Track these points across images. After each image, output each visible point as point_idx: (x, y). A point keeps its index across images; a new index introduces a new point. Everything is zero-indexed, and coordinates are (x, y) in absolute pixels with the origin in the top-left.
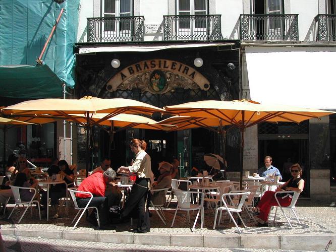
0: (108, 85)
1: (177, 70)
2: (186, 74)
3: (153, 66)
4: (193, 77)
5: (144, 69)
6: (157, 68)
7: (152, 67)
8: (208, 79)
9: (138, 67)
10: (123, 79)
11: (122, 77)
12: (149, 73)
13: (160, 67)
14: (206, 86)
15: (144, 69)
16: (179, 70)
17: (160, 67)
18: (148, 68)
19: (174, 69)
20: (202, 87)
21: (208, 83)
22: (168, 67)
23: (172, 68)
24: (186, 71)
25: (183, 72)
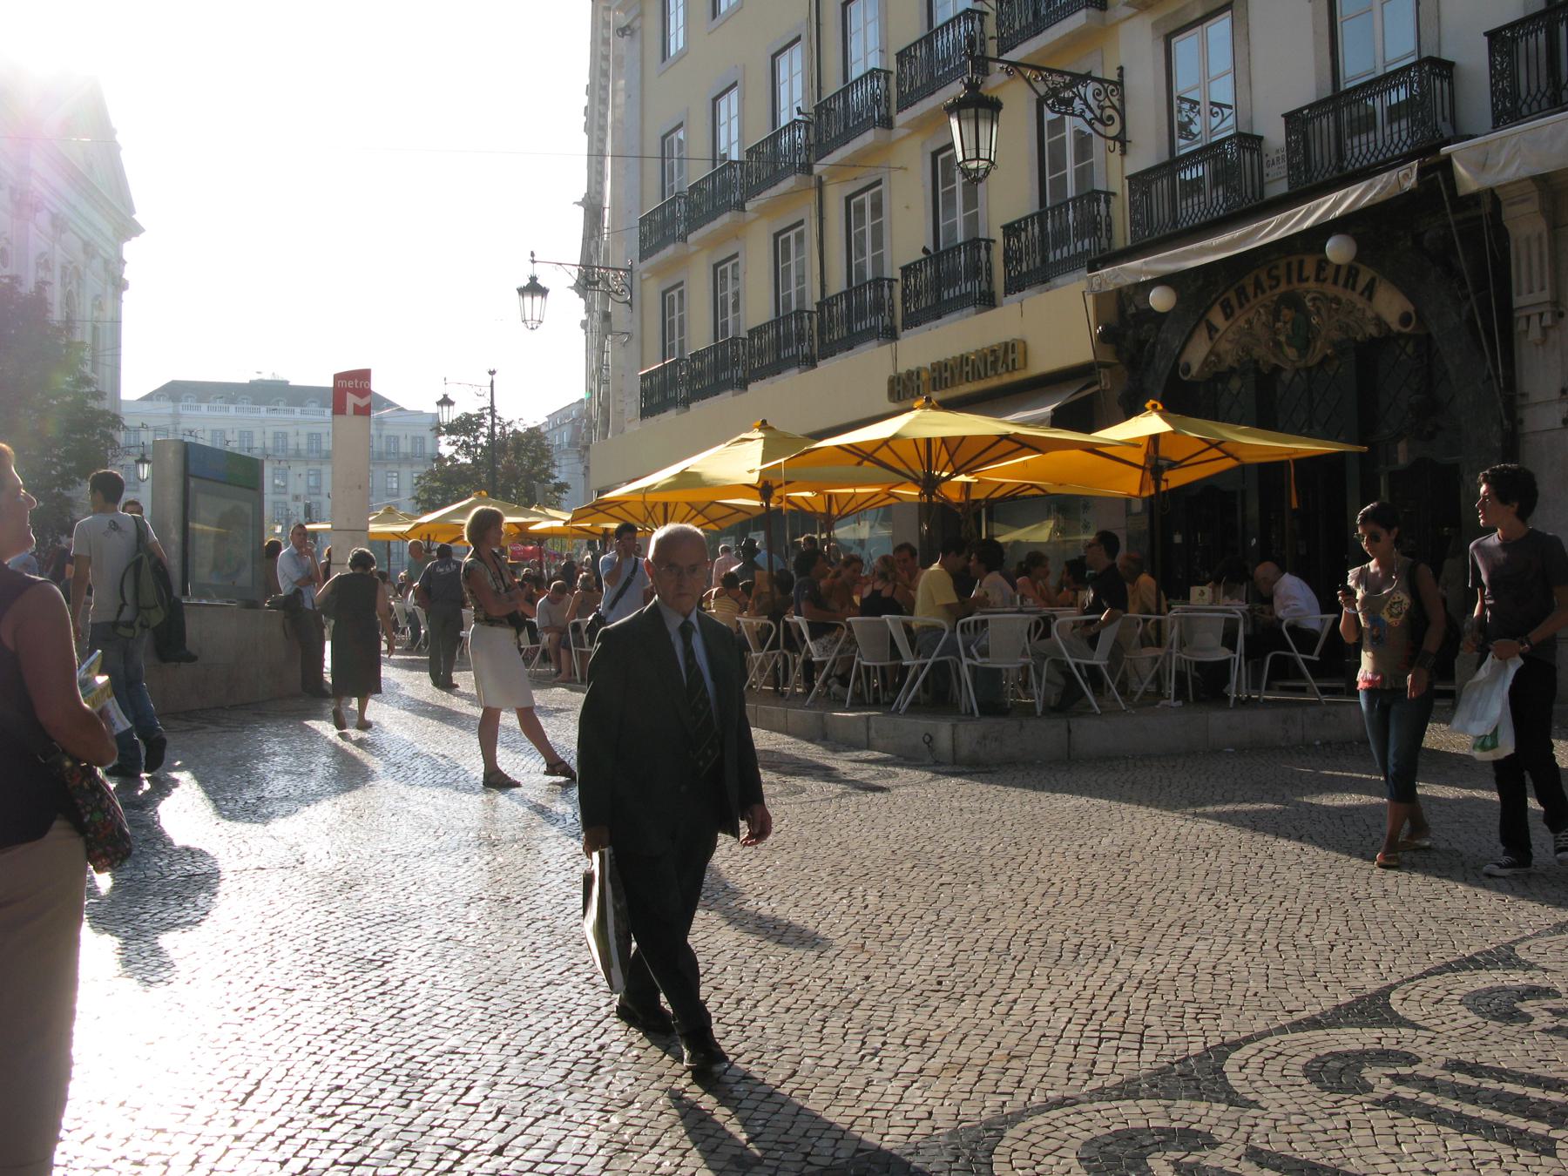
0: (1182, 362)
1: (1330, 280)
2: (1353, 289)
3: (1274, 283)
4: (1370, 298)
5: (1256, 295)
6: (1283, 288)
7: (1271, 288)
8: (1410, 295)
9: (1241, 292)
10: (1211, 338)
11: (1209, 332)
12: (1265, 306)
13: (1289, 281)
14: (1405, 319)
15: (1256, 295)
16: (1335, 282)
17: (1289, 281)
18: (1263, 292)
19: (1325, 280)
20: (1396, 326)
21: (1410, 308)
22: (1307, 279)
23: (1317, 279)
24: (1351, 280)
25: (1346, 286)
